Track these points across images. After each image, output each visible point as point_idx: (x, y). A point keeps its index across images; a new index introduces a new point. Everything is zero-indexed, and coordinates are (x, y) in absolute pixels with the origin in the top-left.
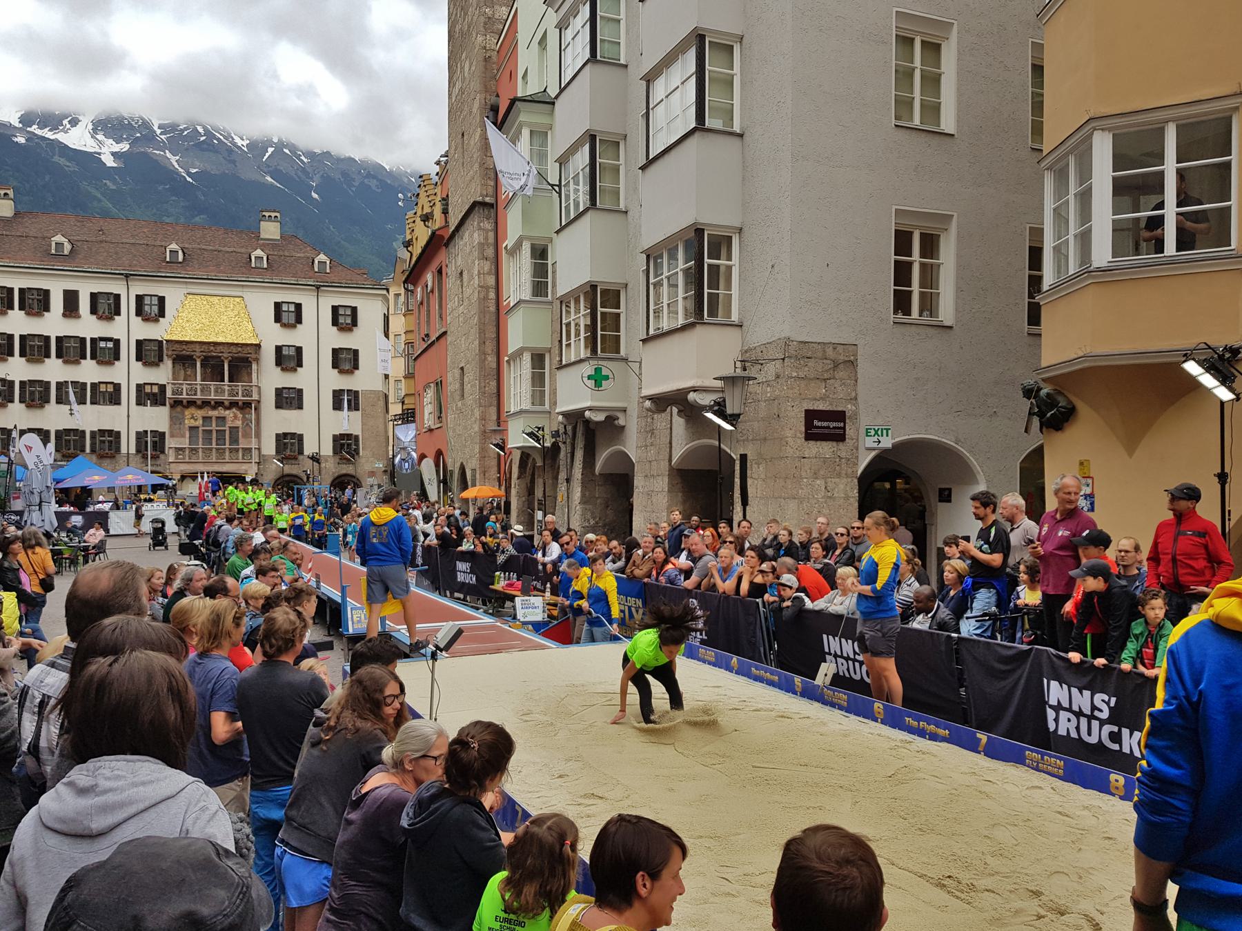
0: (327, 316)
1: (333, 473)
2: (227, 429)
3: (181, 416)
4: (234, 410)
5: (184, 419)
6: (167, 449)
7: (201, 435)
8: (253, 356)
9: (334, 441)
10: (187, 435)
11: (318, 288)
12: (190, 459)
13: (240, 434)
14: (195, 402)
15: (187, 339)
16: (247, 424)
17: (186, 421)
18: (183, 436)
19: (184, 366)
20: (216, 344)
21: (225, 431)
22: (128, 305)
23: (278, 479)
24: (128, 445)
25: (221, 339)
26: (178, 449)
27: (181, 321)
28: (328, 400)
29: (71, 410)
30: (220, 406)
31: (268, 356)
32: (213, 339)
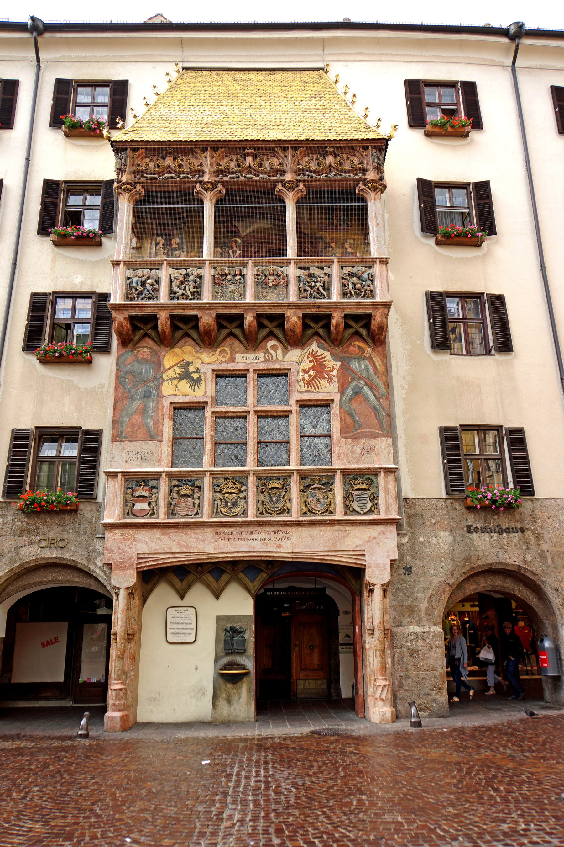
2: (294, 408)
3: (148, 371)
4: (314, 347)
5: (158, 380)
6: (102, 478)
7: (208, 432)
8: (371, 175)
12: (172, 513)
14: (196, 318)
16: (357, 393)
17: (167, 389)
19: (168, 243)
21: (286, 415)
23: (460, 586)
27: (164, 111)
30: (271, 334)
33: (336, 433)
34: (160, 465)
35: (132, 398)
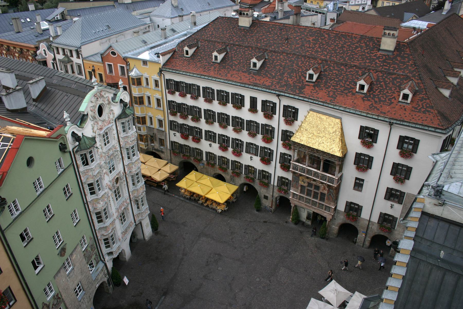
0: (395, 141)
1: (376, 232)
9: (380, 216)
10: (300, 188)
11: (391, 124)
13: (326, 198)
15: (302, 143)
17: (300, 182)
18: (297, 188)
20: (318, 151)
22: (279, 110)
24: (274, 181)
25: (321, 148)
26: (294, 194)
28: (382, 192)
29: (251, 157)
31: (351, 158)
32: (316, 147)
33: (325, 199)
34: (298, 192)
35: (294, 181)
